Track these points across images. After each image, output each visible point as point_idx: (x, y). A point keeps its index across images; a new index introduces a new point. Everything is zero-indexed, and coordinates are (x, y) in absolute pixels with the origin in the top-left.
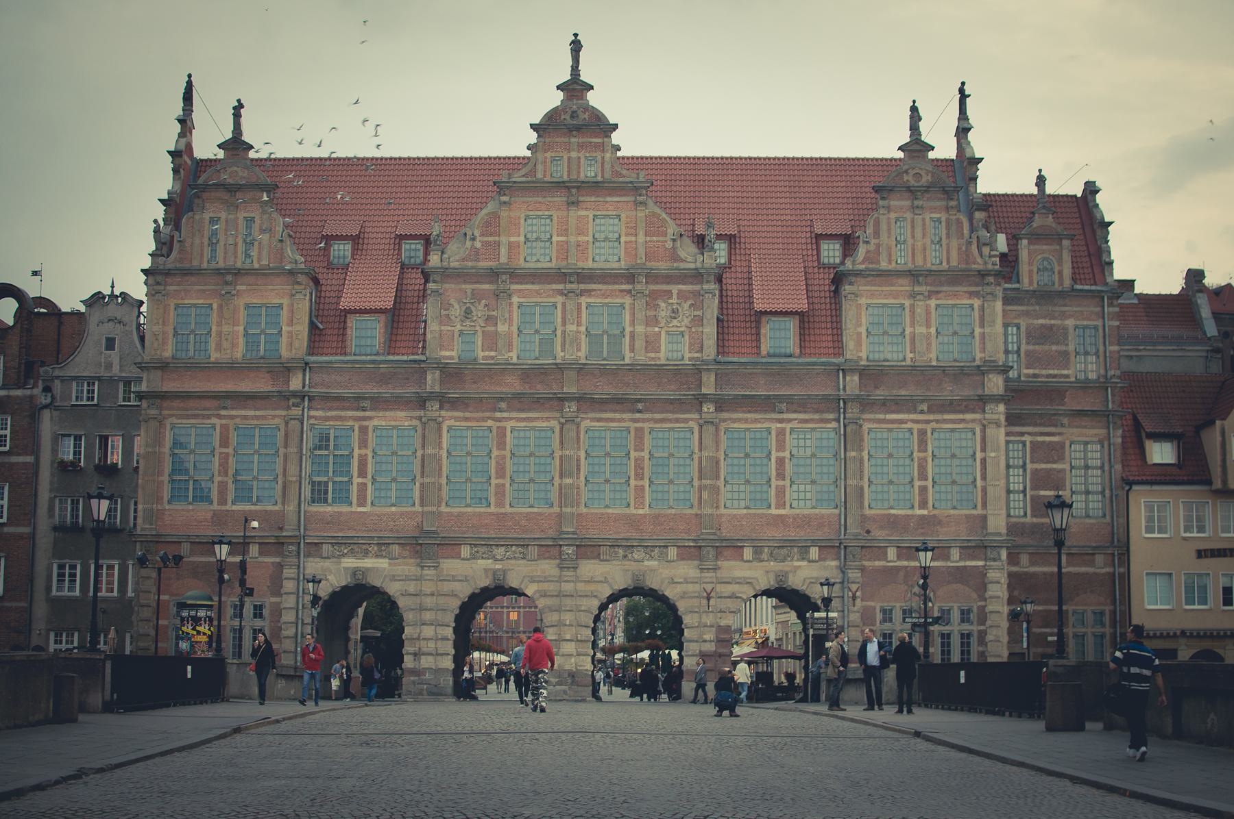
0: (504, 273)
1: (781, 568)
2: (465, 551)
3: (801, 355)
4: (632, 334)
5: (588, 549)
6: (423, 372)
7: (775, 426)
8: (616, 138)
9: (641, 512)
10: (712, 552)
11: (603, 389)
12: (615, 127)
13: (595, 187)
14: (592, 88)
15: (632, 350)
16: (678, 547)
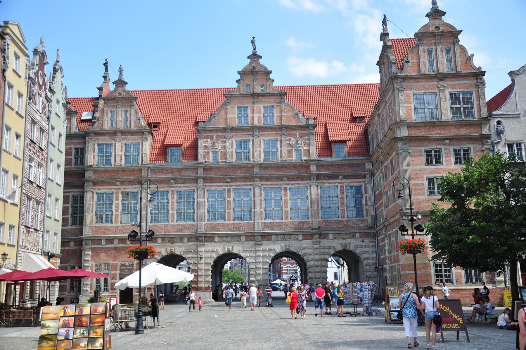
0: (228, 129)
1: (344, 242)
2: (216, 239)
3: (349, 157)
4: (281, 151)
5: (266, 237)
6: (197, 169)
7: (339, 185)
8: (271, 76)
9: (287, 221)
10: (317, 236)
11: (270, 173)
12: (271, 72)
13: (263, 95)
14: (261, 57)
15: (281, 157)
16: (303, 234)
